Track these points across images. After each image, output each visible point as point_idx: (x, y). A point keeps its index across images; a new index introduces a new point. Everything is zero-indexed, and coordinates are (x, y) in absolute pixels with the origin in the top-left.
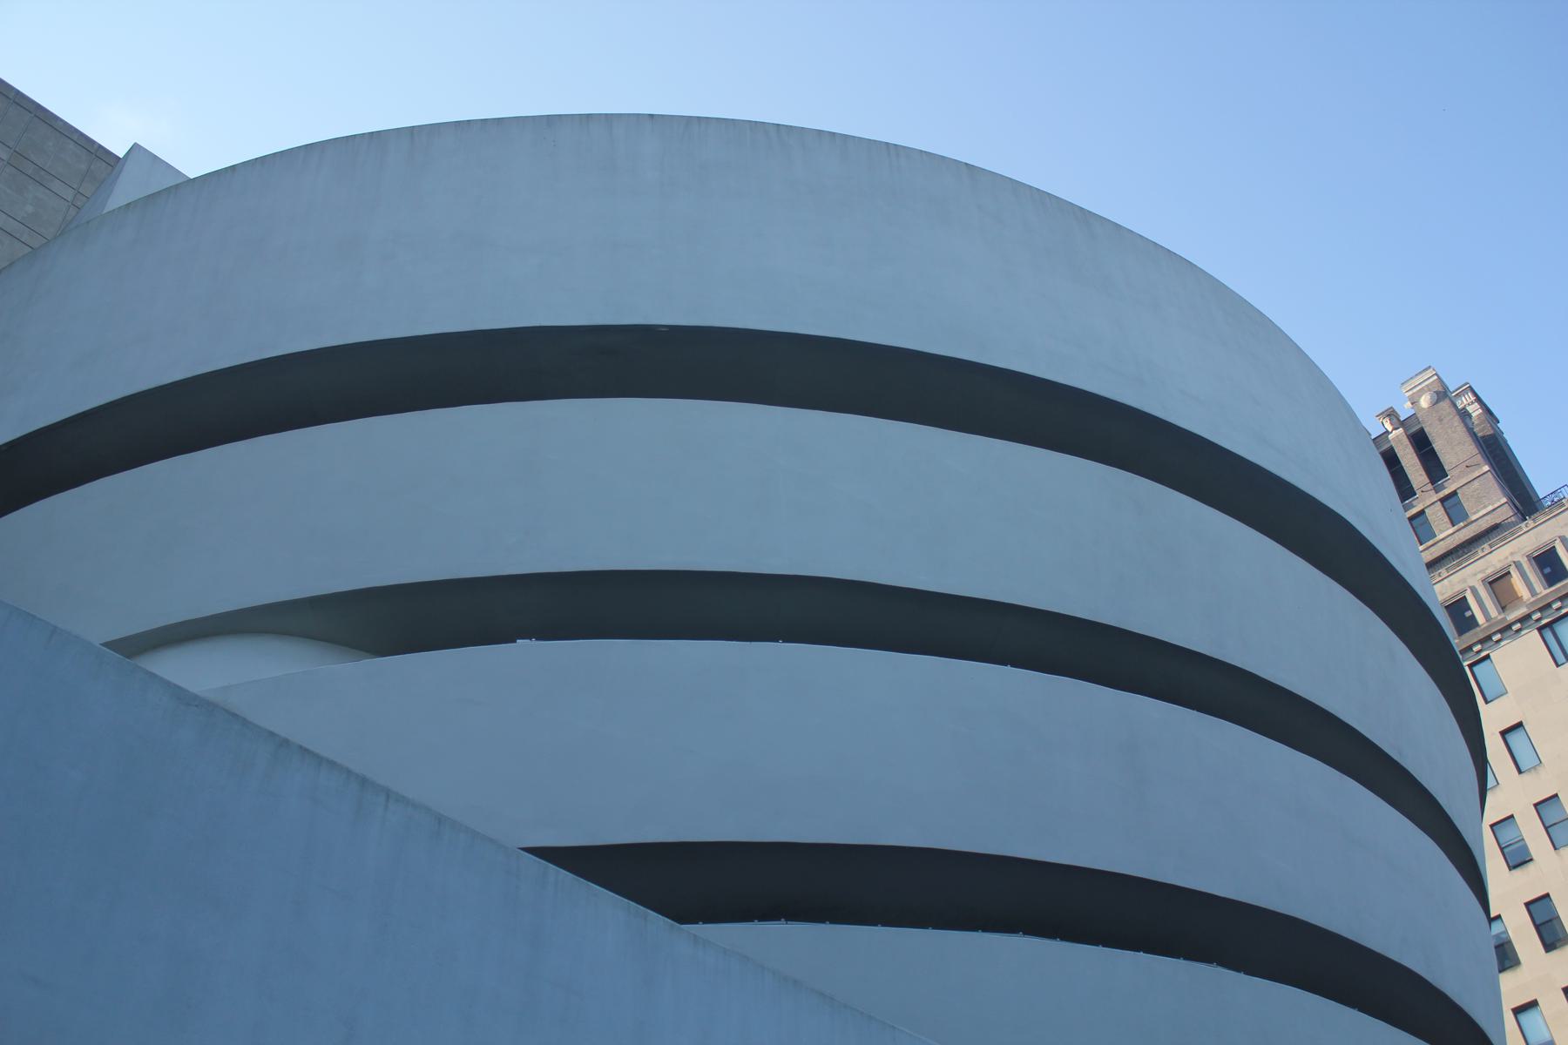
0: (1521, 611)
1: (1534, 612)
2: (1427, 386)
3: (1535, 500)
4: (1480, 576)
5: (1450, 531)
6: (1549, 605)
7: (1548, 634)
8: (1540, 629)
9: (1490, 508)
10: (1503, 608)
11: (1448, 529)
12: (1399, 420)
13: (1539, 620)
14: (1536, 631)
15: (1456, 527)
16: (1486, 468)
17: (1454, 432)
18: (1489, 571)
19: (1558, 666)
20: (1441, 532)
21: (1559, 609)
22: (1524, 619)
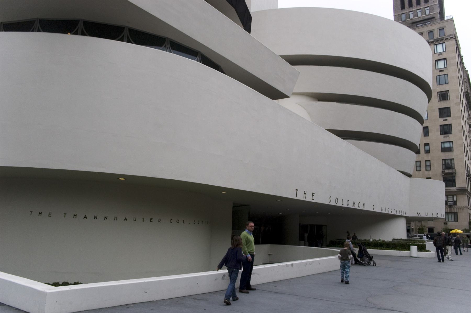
0: (432, 40)
1: (435, 41)
3: (444, 17)
4: (427, 30)
8: (434, 45)
13: (435, 43)
14: (433, 46)
15: (426, 15)
16: (438, 3)
18: (429, 30)
19: (435, 53)
21: (440, 42)
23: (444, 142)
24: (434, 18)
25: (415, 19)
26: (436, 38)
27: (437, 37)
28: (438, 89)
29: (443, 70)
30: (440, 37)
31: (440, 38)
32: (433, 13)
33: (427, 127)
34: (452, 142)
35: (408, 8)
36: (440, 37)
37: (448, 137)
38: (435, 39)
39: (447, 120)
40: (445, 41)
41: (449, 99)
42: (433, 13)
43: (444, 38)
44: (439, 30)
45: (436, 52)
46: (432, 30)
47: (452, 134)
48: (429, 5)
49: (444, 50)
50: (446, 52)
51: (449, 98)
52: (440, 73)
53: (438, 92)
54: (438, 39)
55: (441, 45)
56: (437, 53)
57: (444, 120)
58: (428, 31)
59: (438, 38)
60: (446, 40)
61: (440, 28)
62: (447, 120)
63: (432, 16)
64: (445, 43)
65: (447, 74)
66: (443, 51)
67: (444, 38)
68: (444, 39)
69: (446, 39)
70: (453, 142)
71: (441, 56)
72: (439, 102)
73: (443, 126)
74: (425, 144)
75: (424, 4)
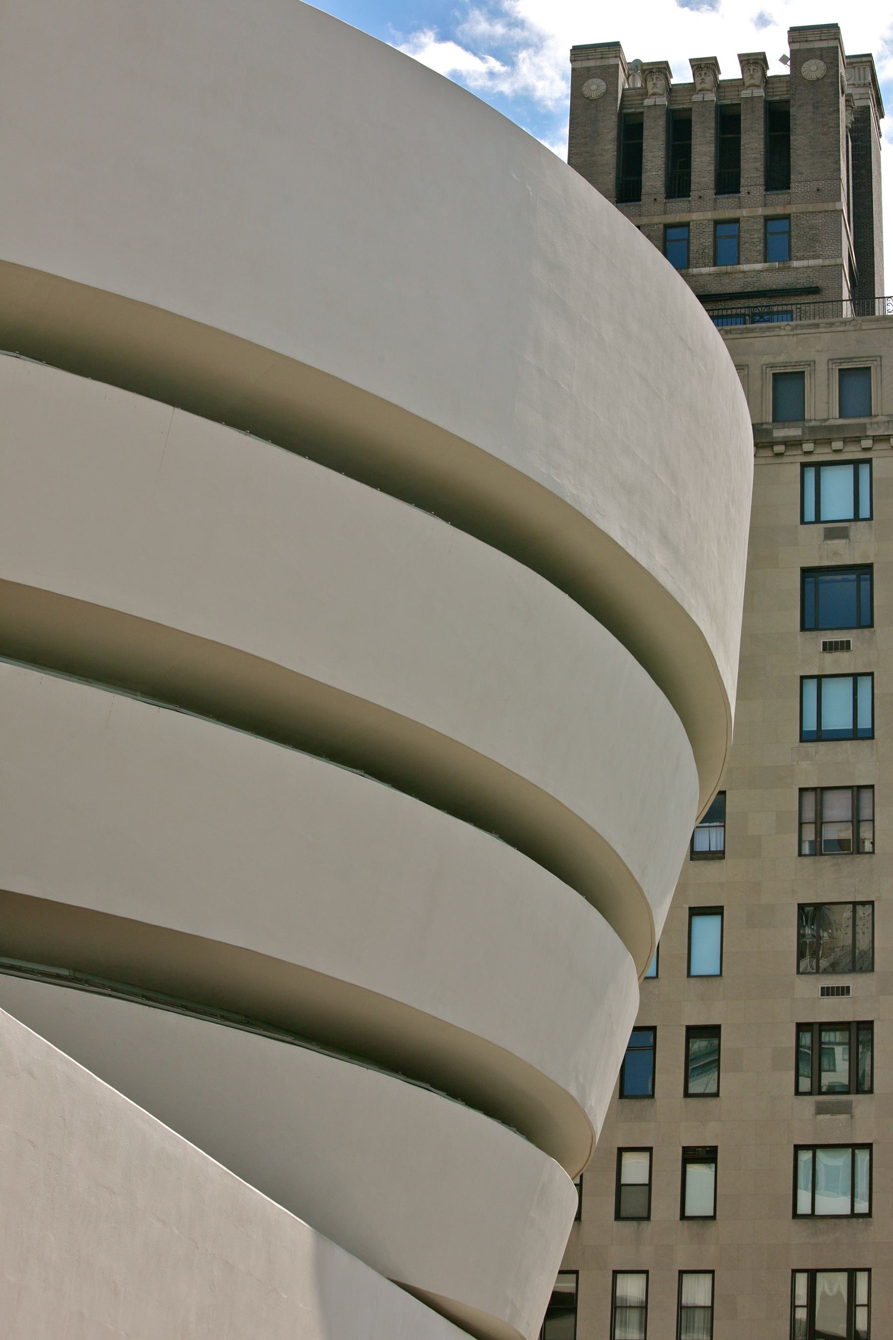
0: (794, 432)
2: (821, 49)
5: (759, 266)
6: (829, 442)
7: (810, 474)
8: (804, 466)
9: (819, 262)
10: (774, 420)
11: (757, 262)
12: (764, 74)
14: (798, 467)
15: (767, 265)
17: (824, 134)
18: (782, 358)
19: (803, 522)
20: (748, 262)
22: (792, 444)
23: (813, 1148)
24: (814, 290)
25: (701, 275)
26: (817, 424)
27: (822, 415)
28: (804, 764)
29: (848, 642)
30: (841, 417)
31: (839, 427)
32: (812, 262)
33: (713, 1031)
34: (868, 1146)
35: (661, 197)
36: (841, 417)
37: (846, 1109)
38: (813, 423)
39: (844, 991)
40: (866, 450)
41: (868, 847)
42: (812, 262)
43: (864, 427)
44: (843, 373)
45: (810, 515)
46: (798, 364)
47: (871, 1091)
48: (792, 209)
49: (864, 512)
50: (873, 522)
51: (873, 843)
52: (829, 657)
53: (802, 790)
54: (830, 428)
55: (847, 472)
56: (818, 520)
57: (827, 992)
58: (772, 366)
59: (831, 422)
60: (880, 446)
61: (849, 359)
62: (844, 991)
63: (803, 282)
64: (869, 461)
65: (871, 674)
66: (857, 518)
67: (869, 433)
68: (867, 437)
69: (876, 439)
70: (874, 1146)
71: (838, 544)
72: (807, 861)
73: (816, 1028)
74: (685, 1149)
75: (759, 191)
